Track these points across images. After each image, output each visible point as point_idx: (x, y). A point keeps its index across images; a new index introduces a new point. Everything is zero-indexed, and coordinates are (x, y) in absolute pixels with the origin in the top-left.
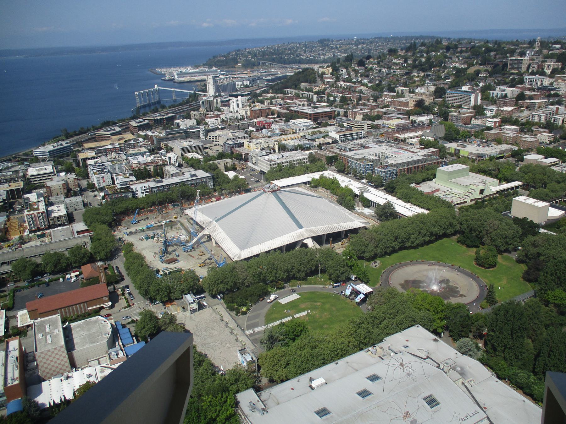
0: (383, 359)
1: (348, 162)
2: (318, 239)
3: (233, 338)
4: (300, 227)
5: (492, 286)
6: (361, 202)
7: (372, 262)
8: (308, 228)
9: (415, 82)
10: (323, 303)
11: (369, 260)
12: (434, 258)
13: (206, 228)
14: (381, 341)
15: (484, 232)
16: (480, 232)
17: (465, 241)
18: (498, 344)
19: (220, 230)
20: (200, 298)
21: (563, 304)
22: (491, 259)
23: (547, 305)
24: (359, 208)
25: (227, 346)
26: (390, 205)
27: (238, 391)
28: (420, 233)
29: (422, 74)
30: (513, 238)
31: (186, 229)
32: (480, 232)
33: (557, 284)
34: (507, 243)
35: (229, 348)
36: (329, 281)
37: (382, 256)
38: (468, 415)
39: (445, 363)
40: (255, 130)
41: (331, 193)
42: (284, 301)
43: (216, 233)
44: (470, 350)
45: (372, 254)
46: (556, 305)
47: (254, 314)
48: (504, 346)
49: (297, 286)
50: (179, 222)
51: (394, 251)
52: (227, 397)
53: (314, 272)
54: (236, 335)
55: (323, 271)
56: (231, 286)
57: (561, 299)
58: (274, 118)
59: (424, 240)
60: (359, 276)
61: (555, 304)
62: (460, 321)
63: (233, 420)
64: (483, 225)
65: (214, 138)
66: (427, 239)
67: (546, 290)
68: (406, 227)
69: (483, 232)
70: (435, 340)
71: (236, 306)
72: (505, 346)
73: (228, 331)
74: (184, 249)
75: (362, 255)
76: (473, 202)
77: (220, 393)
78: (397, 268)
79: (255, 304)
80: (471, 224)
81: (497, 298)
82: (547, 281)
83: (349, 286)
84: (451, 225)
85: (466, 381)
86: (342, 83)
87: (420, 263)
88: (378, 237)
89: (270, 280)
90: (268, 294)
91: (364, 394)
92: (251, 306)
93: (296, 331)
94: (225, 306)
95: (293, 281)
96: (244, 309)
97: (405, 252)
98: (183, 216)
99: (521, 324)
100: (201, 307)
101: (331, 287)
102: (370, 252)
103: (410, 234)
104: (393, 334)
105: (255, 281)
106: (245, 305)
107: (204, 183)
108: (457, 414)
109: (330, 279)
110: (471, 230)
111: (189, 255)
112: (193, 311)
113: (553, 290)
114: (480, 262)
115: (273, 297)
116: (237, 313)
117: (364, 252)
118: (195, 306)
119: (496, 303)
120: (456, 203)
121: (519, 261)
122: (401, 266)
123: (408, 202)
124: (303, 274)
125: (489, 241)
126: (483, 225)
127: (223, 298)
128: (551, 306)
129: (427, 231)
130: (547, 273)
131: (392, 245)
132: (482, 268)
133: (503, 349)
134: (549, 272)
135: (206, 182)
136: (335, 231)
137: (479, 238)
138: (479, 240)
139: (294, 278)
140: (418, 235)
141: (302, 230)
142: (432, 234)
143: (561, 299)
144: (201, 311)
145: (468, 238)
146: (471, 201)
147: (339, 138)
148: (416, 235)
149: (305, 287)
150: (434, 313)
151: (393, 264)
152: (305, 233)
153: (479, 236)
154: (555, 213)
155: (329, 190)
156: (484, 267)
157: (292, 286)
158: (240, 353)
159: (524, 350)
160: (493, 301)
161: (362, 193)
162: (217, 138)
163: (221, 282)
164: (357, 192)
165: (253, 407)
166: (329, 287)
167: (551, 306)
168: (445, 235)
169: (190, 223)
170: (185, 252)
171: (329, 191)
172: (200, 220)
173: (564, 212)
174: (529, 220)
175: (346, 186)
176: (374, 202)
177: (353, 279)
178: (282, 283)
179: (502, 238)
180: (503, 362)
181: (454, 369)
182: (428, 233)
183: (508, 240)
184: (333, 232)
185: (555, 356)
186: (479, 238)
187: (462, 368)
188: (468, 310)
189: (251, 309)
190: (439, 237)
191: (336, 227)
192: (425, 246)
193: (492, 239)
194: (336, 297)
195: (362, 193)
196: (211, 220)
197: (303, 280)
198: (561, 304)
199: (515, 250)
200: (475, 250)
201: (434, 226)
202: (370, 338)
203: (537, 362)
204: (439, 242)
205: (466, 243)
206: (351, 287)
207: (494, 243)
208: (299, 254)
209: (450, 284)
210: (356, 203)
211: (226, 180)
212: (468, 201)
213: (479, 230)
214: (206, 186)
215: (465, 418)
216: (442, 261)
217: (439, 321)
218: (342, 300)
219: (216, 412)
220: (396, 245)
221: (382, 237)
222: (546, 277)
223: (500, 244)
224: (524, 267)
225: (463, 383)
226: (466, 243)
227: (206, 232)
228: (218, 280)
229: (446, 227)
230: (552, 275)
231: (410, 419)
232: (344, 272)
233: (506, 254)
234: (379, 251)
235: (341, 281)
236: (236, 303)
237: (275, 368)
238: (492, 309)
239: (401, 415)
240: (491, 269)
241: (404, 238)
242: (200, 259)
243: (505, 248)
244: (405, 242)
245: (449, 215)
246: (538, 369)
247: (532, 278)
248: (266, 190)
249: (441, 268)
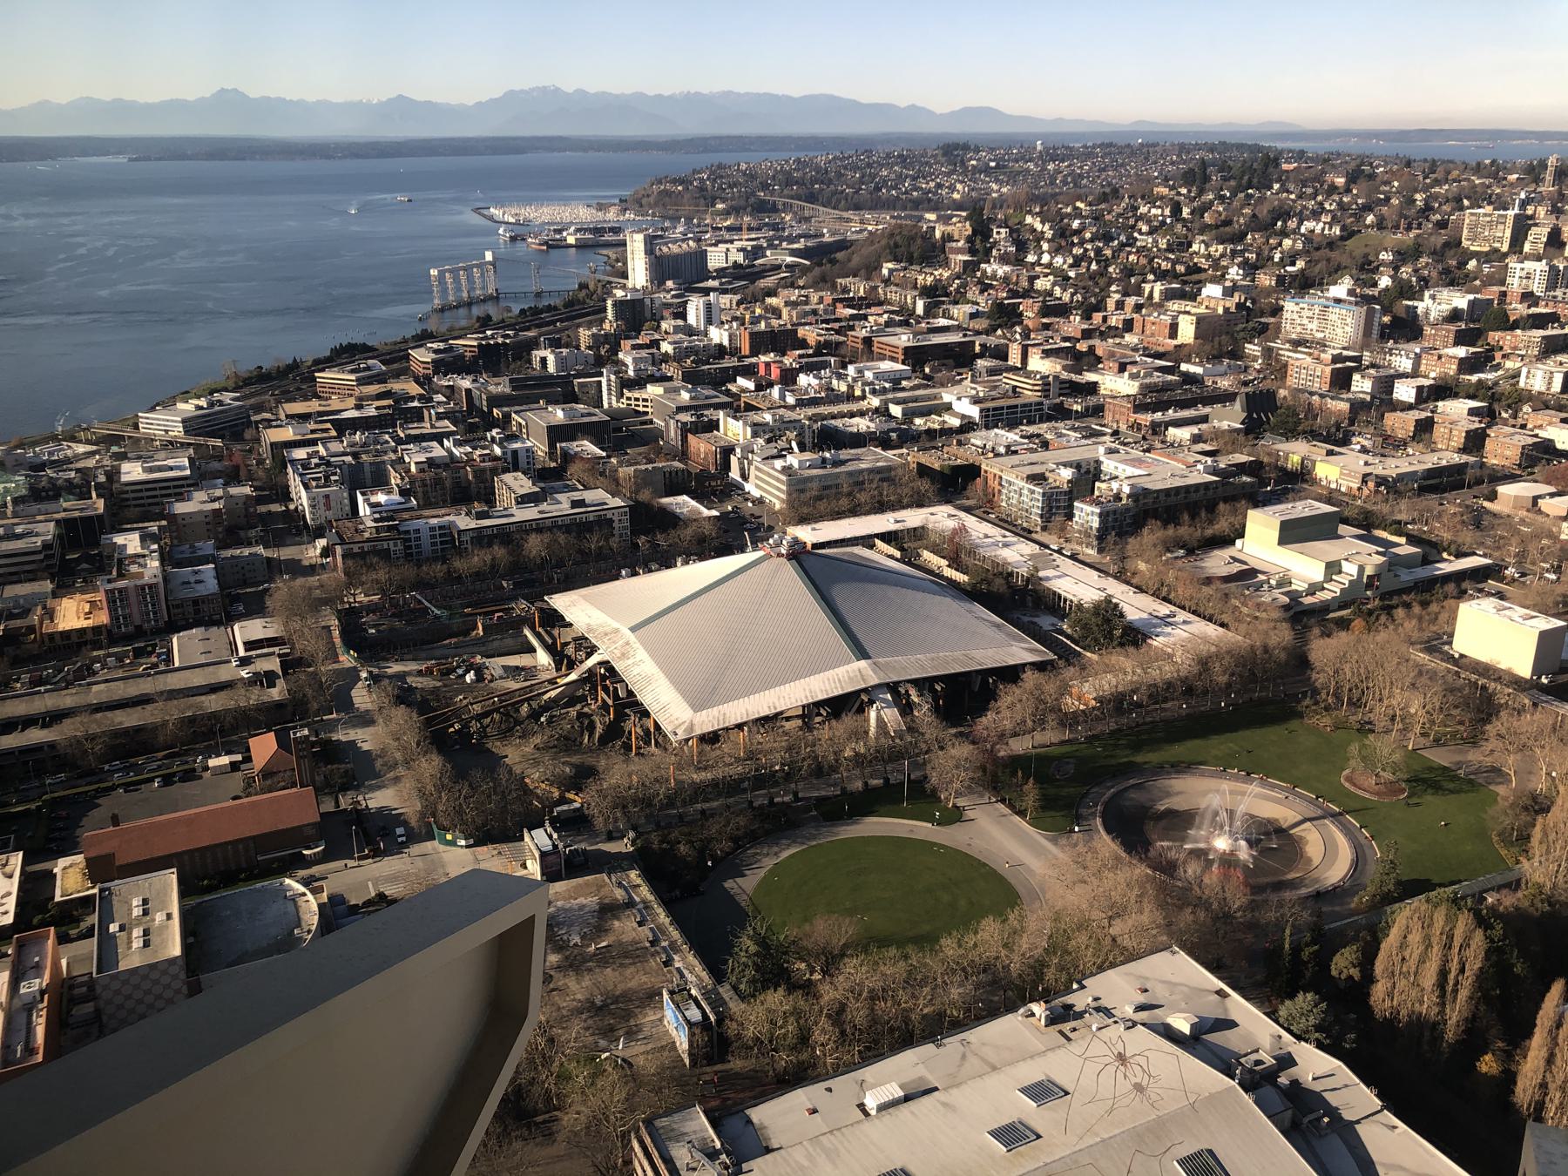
0: (1069, 1039)
1: (1000, 484)
4: (862, 653)
9: (1199, 270)
19: (641, 654)
29: (1217, 249)
40: (751, 385)
43: (630, 662)
65: (641, 403)
86: (995, 266)
91: (1012, 1135)
141: (863, 664)
147: (981, 417)
162: (649, 404)
172: (589, 625)
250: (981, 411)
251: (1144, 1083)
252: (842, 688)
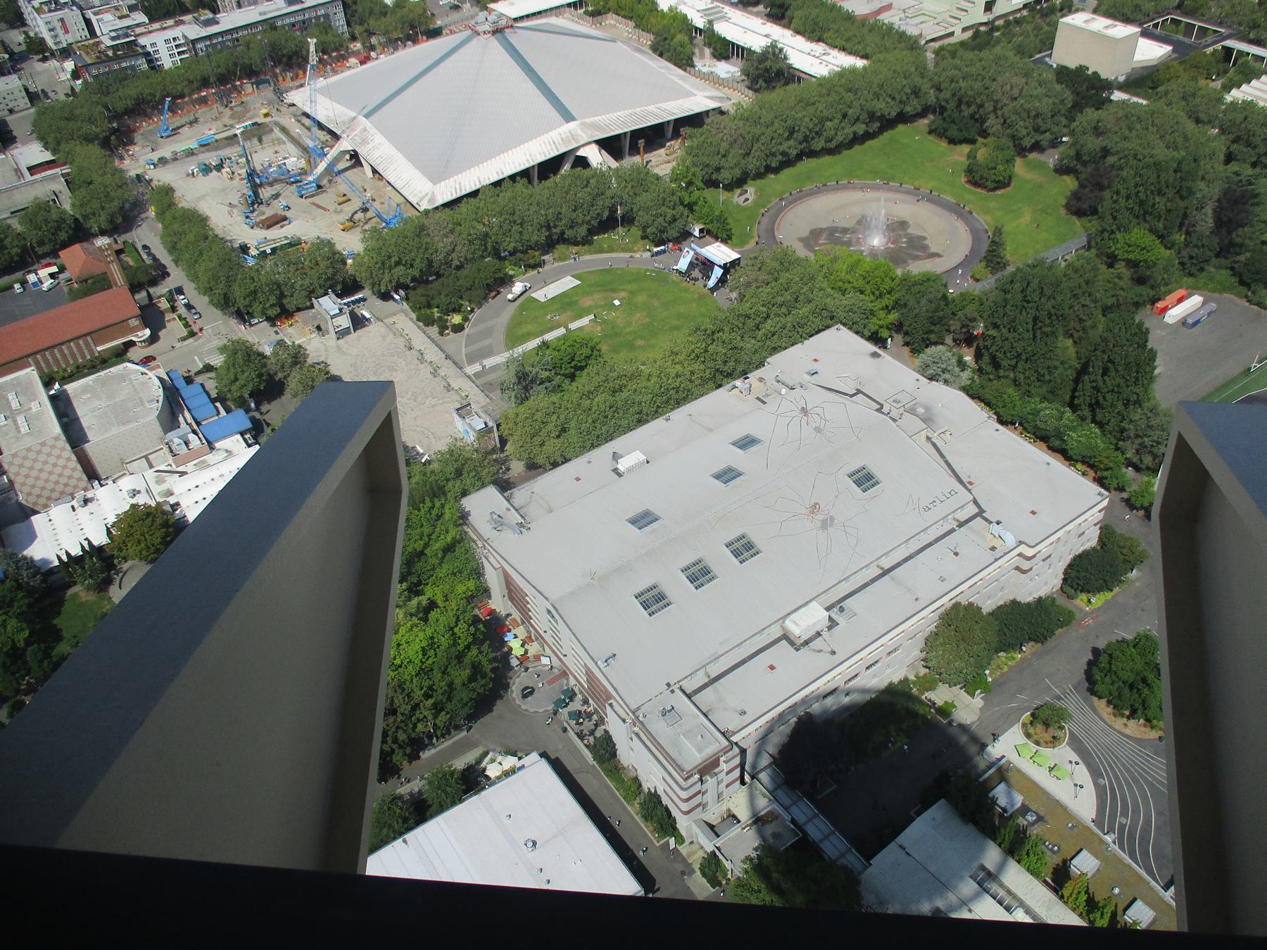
0: (764, 403)
2: (611, 145)
3: (438, 385)
4: (568, 117)
5: (998, 231)
6: (709, 45)
7: (738, 191)
8: (588, 120)
10: (631, 292)
11: (729, 188)
12: (875, 173)
13: (344, 136)
14: (761, 364)
15: (989, 107)
16: (981, 106)
17: (946, 130)
18: (1005, 353)
19: (379, 138)
20: (354, 302)
21: (1146, 261)
22: (1001, 167)
23: (1111, 266)
24: (705, 63)
25: (428, 402)
26: (777, 51)
27: (465, 493)
28: (845, 116)
30: (1052, 116)
31: (296, 142)
32: (981, 106)
33: (1137, 217)
34: (1037, 129)
35: (433, 406)
36: (642, 242)
37: (759, 176)
39: (894, 401)
41: (637, 26)
42: (542, 295)
43: (370, 146)
44: (943, 372)
45: (737, 173)
46: (1133, 264)
47: (480, 327)
48: (1016, 357)
49: (570, 258)
50: (277, 124)
51: (788, 163)
52: (443, 506)
53: (608, 224)
54: (444, 378)
55: (628, 220)
56: (421, 270)
57: (1143, 249)
59: (855, 133)
60: (709, 227)
61: (1128, 261)
62: (927, 311)
63: (459, 550)
64: (987, 88)
66: (860, 129)
67: (1112, 232)
68: (813, 104)
69: (986, 105)
70: (875, 355)
71: (437, 315)
72: (1019, 355)
73: (425, 370)
74: (299, 192)
75: (714, 177)
76: (969, 34)
77: (427, 500)
78: (791, 203)
79: (480, 305)
80: (960, 88)
81: (1008, 257)
82: (1116, 211)
83: (687, 249)
84: (916, 92)
85: (936, 434)
87: (845, 188)
88: (749, 133)
89: (510, 248)
90: (507, 281)
91: (727, 475)
92: (472, 311)
93: (577, 359)
94: (414, 316)
95: (561, 248)
96: (457, 319)
97: (807, 164)
98: (284, 109)
99: (1054, 307)
100: (358, 322)
101: (649, 254)
102: (732, 168)
103: (822, 121)
104: (786, 348)
105: (474, 253)
106: (457, 310)
107: (322, 20)
109: (643, 238)
110: (960, 102)
111: (314, 204)
112: (342, 334)
113: (1127, 229)
114: (978, 178)
115: (518, 287)
116: (443, 329)
117: (718, 169)
118: (345, 321)
119: (1005, 266)
120: (929, 38)
121: (1061, 170)
122: (802, 196)
123: (819, 40)
124: (582, 231)
125: (1000, 126)
126: (987, 88)
127: (407, 299)
128: (1121, 267)
129: (862, 109)
130: (1118, 193)
131: (781, 148)
132: (979, 190)
133: (1013, 363)
134: (1123, 192)
135: (326, 16)
136: (649, 124)
137: (977, 120)
138: (978, 125)
139: (562, 239)
140: (841, 122)
141: (572, 125)
142: (872, 116)
143: (1143, 249)
144: (359, 332)
145: (953, 121)
146: (964, 30)
148: (836, 121)
149: (590, 260)
150: (873, 298)
151: (784, 193)
152: (580, 132)
153: (977, 116)
154: (1151, 52)
155: (631, 19)
156: (984, 187)
157: (561, 259)
158: (460, 416)
159: (1057, 364)
160: (998, 263)
161: (711, 22)
163: (398, 263)
164: (700, 22)
165: (499, 522)
166: (643, 256)
167: (1121, 267)
168: (903, 118)
169: (303, 125)
170: (301, 197)
171: (631, 24)
172: (328, 116)
173: (1169, 48)
174: (1090, 72)
175: (671, 9)
176: (738, 46)
177: (697, 233)
178: (536, 253)
179: (1029, 117)
180: (1011, 391)
181: (912, 411)
182: (864, 116)
183: (1039, 121)
184: (645, 125)
185: (1117, 371)
186: (977, 120)
187: (927, 409)
188: (946, 286)
189: (472, 317)
190: (888, 124)
192: (857, 148)
193: (1005, 122)
194: (661, 277)
195: (711, 22)
196: (353, 114)
197: (584, 245)
198: (1140, 261)
199: (1055, 144)
200: (966, 148)
201: (877, 96)
202: (736, 361)
203: (1080, 385)
204: (887, 135)
205: (949, 134)
206: (692, 253)
207: (1009, 131)
208: (570, 185)
209: (910, 231)
210: (696, 51)
211: (377, 9)
212: (958, 32)
213: (978, 100)
214: (330, 26)
215: (931, 506)
216: (893, 179)
217: (882, 314)
218: (673, 281)
219: (421, 539)
220: (792, 147)
221: (757, 130)
222: (1115, 202)
223: (1024, 132)
224: (1070, 183)
225: (928, 438)
226: (949, 134)
227: (344, 145)
228: (390, 257)
229: (904, 98)
230: (1128, 198)
231: (820, 517)
232: (675, 220)
233: (1033, 156)
234: (753, 164)
235: (669, 241)
236: (438, 307)
237: (537, 440)
238: (996, 281)
240: (999, 192)
241: (810, 131)
242: (341, 211)
243: (1033, 141)
244: (813, 138)
245: (913, 69)
246: (1081, 400)
247: (1085, 206)
248: (480, 29)
249: (890, 195)
252: (558, 150)
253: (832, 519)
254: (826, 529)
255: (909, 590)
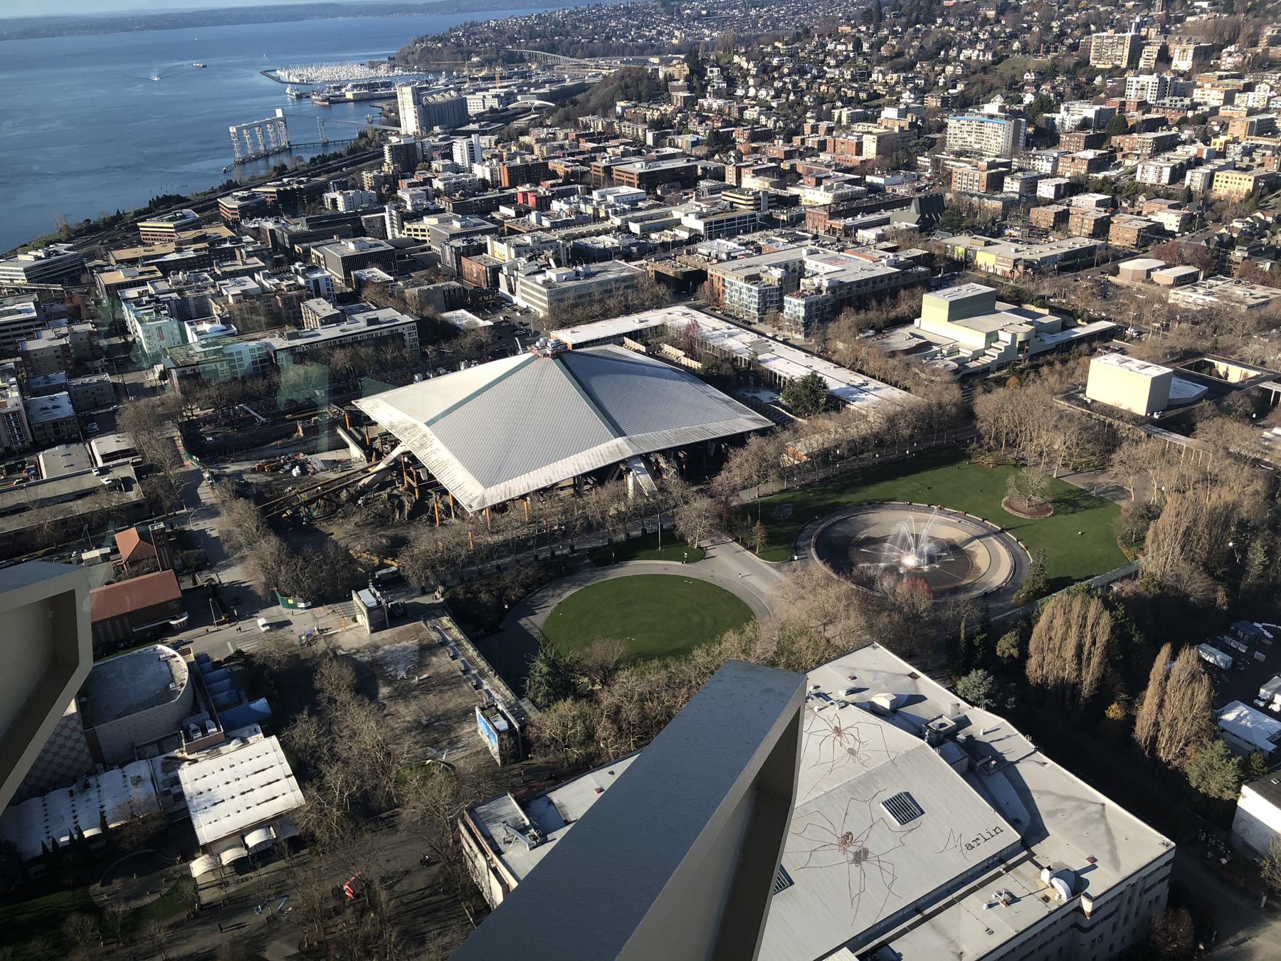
1: (724, 285)
4: (619, 432)
19: (437, 443)
38: (979, 837)
40: (512, 213)
43: (428, 451)
58: (559, 185)
65: (419, 233)
86: (710, 100)
108: (957, 836)
141: (620, 440)
147: (706, 230)
162: (426, 233)
172: (391, 423)
191: (694, 432)
239: (835, 841)
250: (705, 225)
251: (856, 748)
252: (604, 461)
253: (866, 852)
254: (859, 863)
255: (952, 942)
